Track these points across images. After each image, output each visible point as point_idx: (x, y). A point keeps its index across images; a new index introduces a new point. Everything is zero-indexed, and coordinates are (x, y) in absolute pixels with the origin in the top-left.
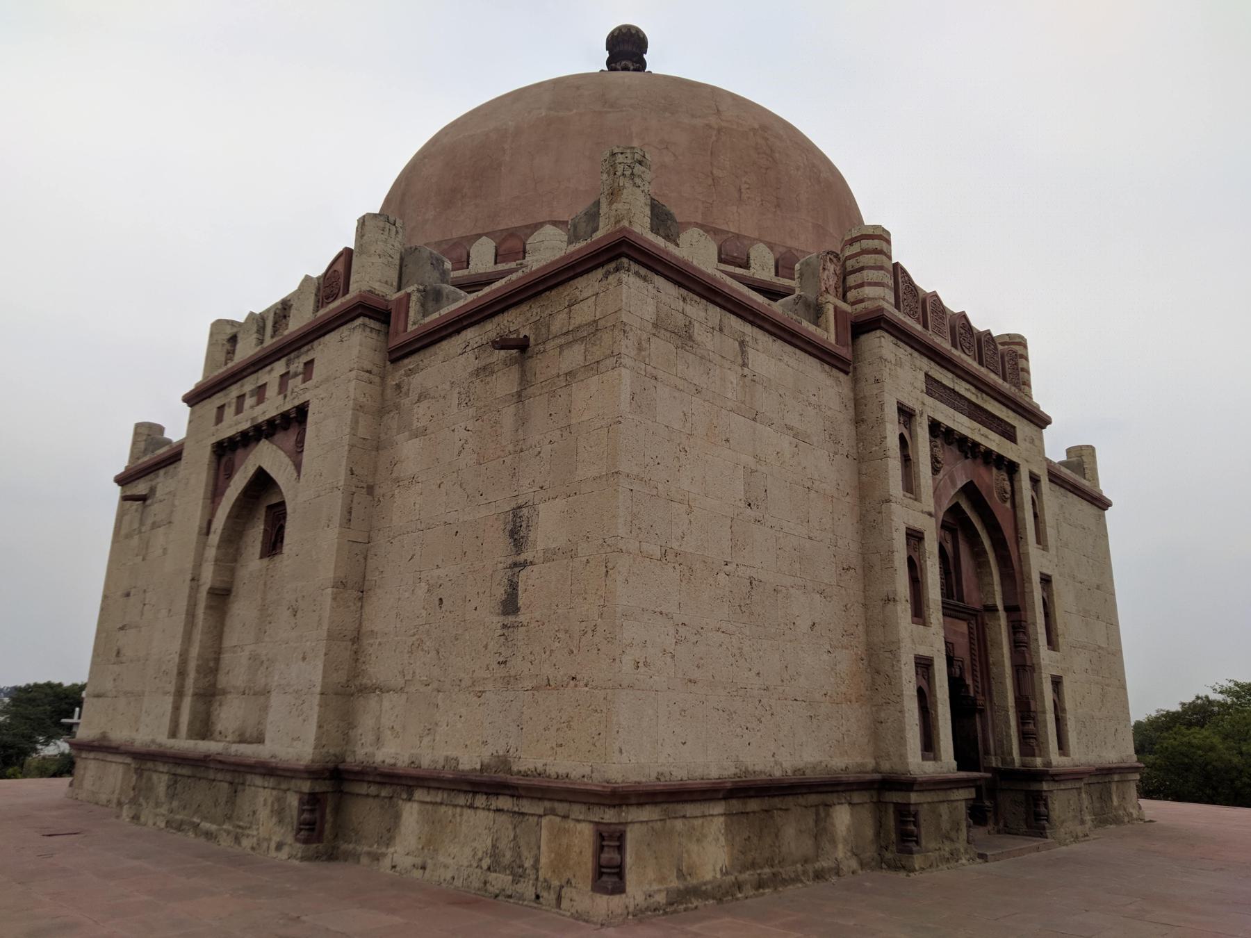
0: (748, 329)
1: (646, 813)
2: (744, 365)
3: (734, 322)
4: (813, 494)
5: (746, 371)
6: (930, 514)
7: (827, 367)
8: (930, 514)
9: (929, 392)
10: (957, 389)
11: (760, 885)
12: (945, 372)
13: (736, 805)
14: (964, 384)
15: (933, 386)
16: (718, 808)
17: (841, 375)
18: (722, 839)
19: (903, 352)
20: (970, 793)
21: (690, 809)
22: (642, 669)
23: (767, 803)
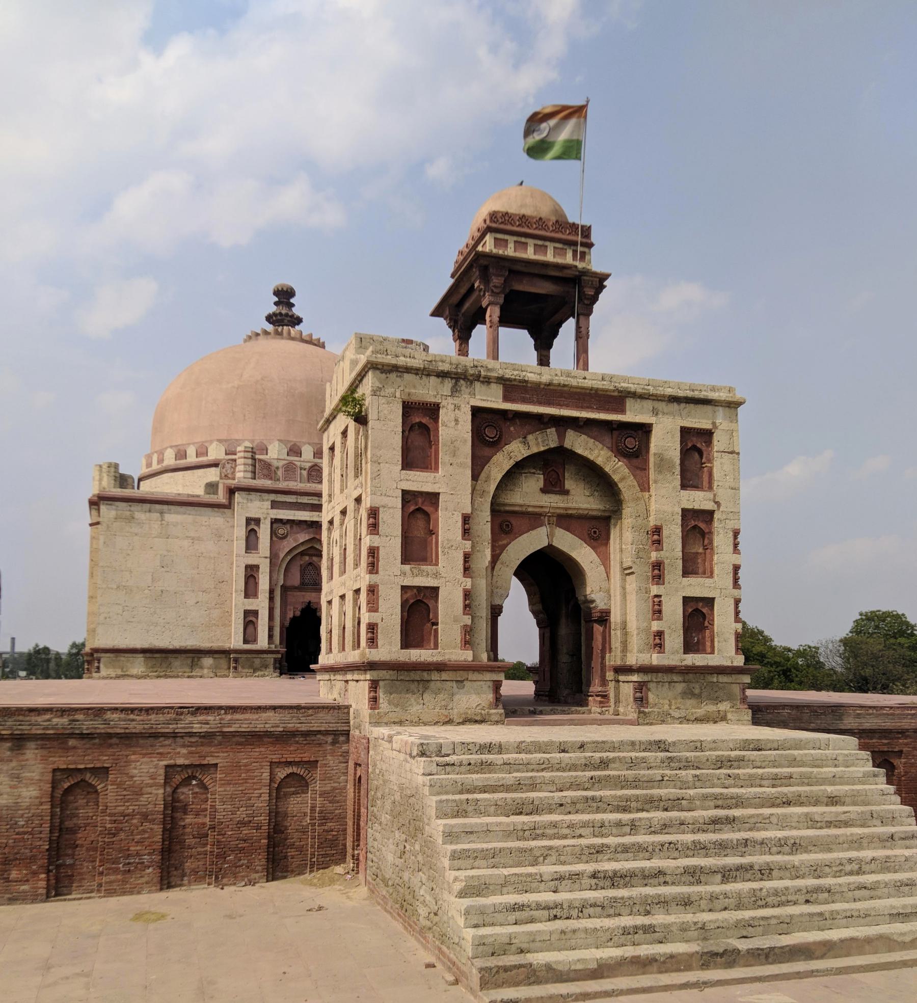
0: (165, 507)
1: (108, 655)
2: (162, 520)
3: (158, 507)
4: (201, 558)
5: (163, 522)
6: (266, 558)
7: (216, 509)
8: (266, 558)
9: (272, 508)
10: (299, 501)
11: (158, 677)
12: (289, 496)
13: (148, 655)
14: (307, 497)
15: (275, 505)
16: (141, 655)
17: (226, 510)
18: (142, 664)
19: (254, 495)
20: (280, 656)
21: (126, 655)
22: (108, 619)
23: (164, 655)
